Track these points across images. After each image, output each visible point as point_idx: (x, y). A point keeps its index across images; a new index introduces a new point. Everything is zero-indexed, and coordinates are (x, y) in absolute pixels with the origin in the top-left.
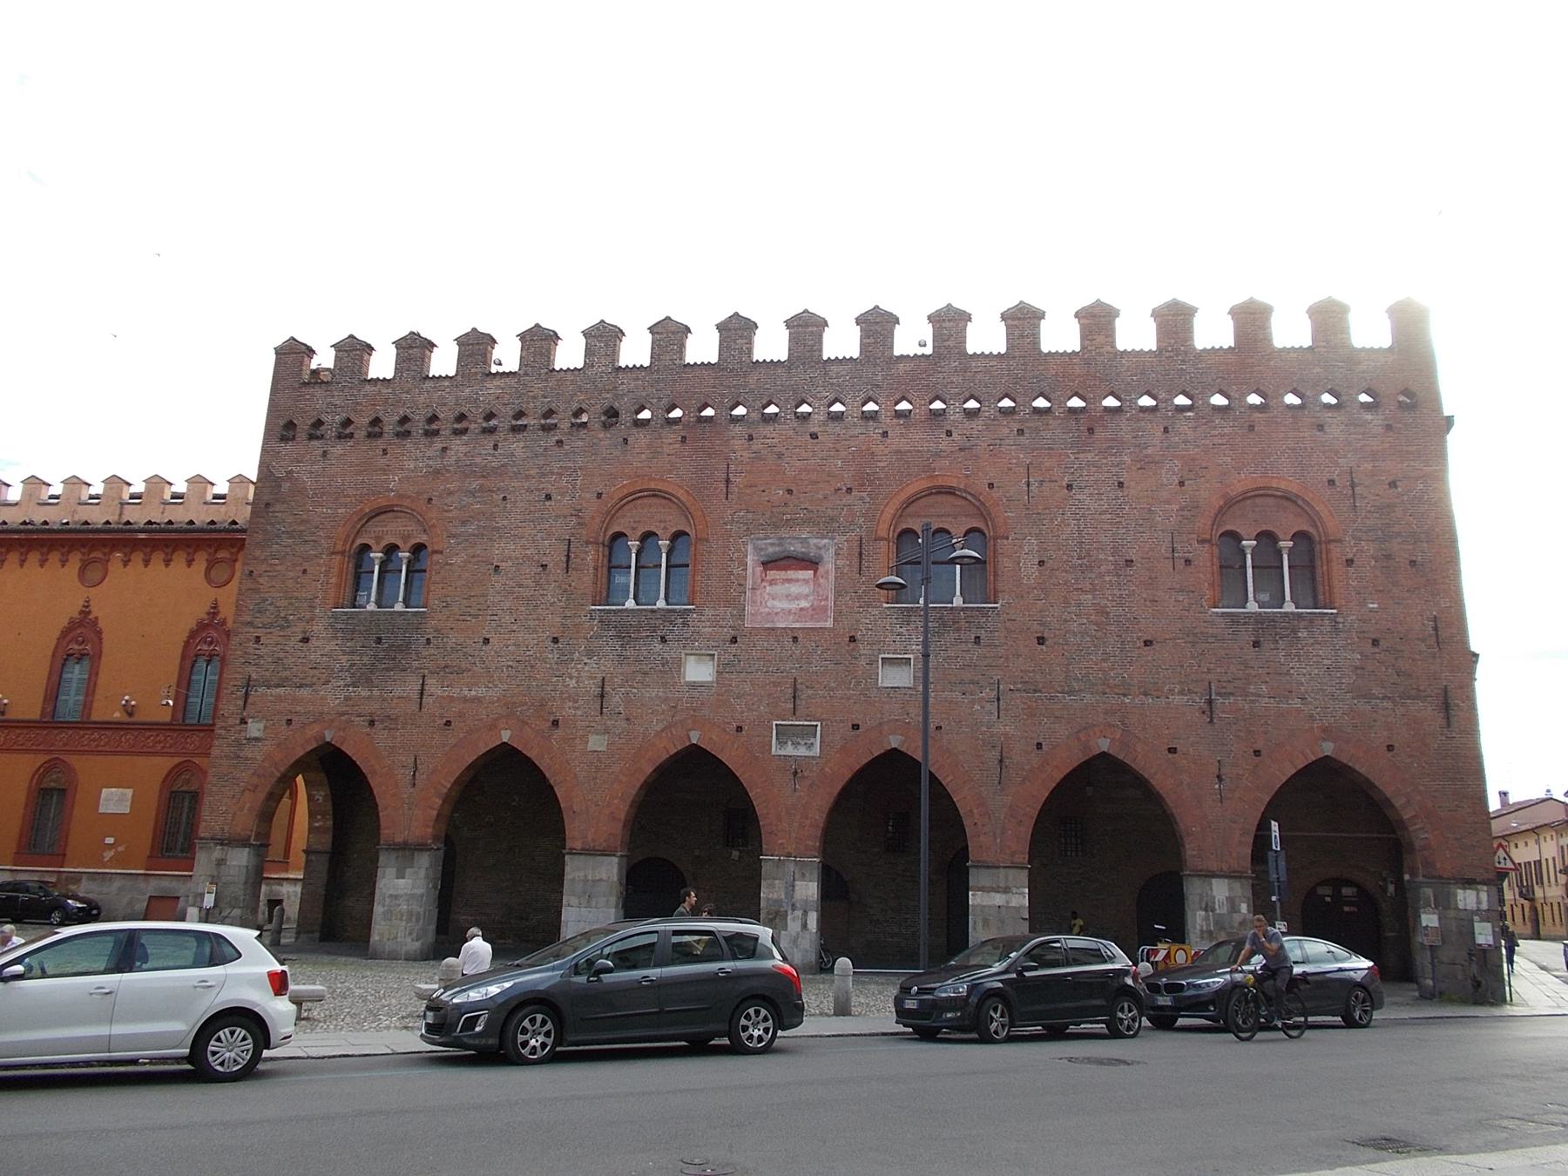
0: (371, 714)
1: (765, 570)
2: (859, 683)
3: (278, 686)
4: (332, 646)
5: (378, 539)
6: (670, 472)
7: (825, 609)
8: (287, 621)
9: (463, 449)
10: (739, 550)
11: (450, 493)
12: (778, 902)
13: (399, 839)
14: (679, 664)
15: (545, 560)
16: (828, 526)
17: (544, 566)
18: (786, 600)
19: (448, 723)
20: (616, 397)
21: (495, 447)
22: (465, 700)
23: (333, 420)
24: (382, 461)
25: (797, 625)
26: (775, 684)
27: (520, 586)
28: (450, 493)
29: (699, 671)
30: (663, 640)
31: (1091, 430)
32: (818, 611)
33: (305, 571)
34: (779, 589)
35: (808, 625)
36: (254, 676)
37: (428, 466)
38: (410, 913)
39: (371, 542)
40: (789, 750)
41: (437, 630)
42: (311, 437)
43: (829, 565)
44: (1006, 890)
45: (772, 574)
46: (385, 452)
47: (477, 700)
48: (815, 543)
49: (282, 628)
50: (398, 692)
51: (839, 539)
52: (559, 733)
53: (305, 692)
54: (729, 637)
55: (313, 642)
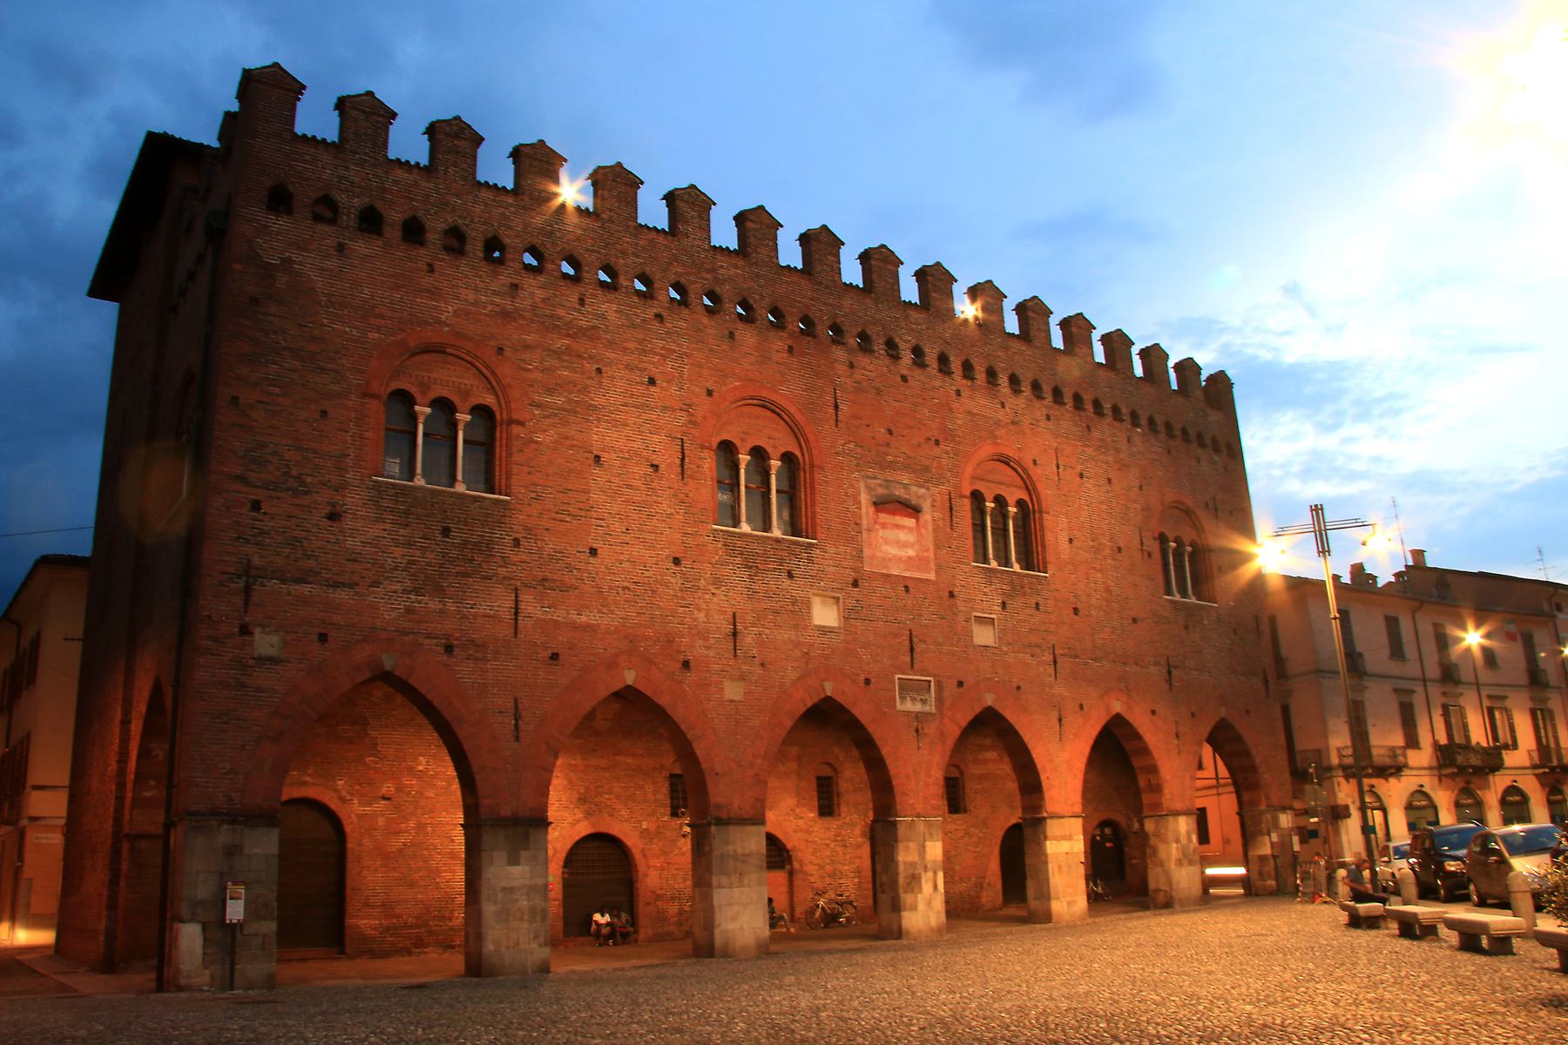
0: (448, 636)
1: (877, 511)
2: (959, 640)
3: (299, 581)
4: (375, 531)
5: (425, 387)
6: (781, 383)
7: (926, 560)
8: (303, 483)
9: (540, 294)
10: (852, 486)
11: (527, 347)
12: (913, 864)
13: (506, 811)
14: (809, 606)
15: (656, 460)
16: (924, 474)
17: (656, 467)
18: (898, 546)
19: (555, 657)
20: (717, 280)
21: (582, 302)
22: (576, 627)
23: (351, 203)
24: (428, 280)
25: (907, 574)
26: (896, 635)
27: (629, 486)
28: (527, 347)
29: (825, 615)
30: (790, 575)
31: (1089, 428)
32: (920, 562)
33: (324, 413)
34: (890, 534)
35: (917, 575)
36: (256, 561)
37: (492, 303)
38: (533, 910)
39: (413, 390)
40: (909, 706)
41: (527, 529)
42: (317, 218)
43: (927, 516)
44: (1069, 838)
45: (883, 517)
46: (431, 269)
47: (589, 628)
48: (916, 493)
49: (296, 493)
50: (483, 608)
51: (935, 490)
52: (691, 677)
53: (342, 595)
54: (851, 580)
55: (348, 522)
